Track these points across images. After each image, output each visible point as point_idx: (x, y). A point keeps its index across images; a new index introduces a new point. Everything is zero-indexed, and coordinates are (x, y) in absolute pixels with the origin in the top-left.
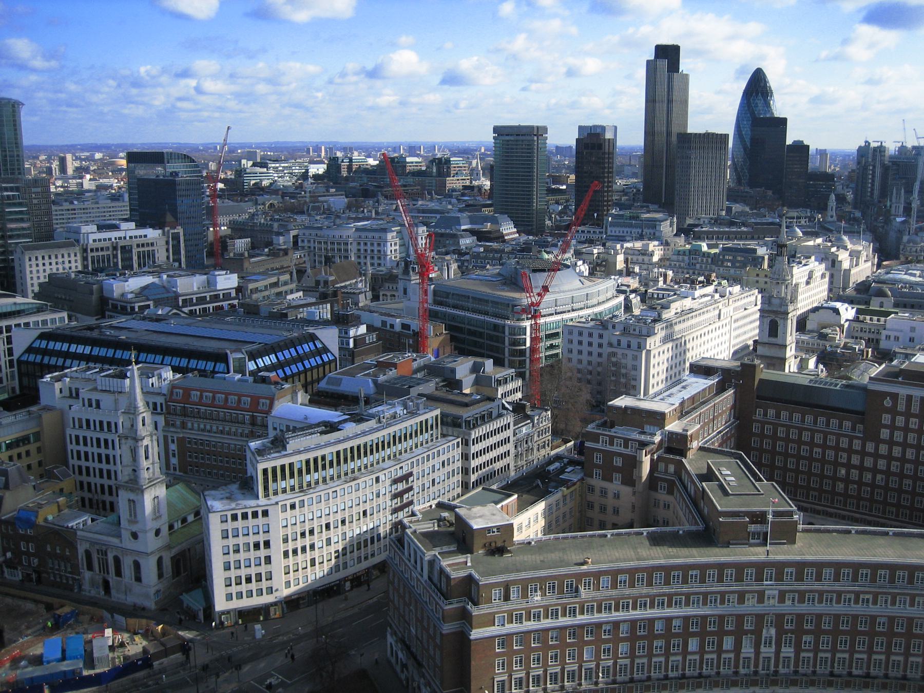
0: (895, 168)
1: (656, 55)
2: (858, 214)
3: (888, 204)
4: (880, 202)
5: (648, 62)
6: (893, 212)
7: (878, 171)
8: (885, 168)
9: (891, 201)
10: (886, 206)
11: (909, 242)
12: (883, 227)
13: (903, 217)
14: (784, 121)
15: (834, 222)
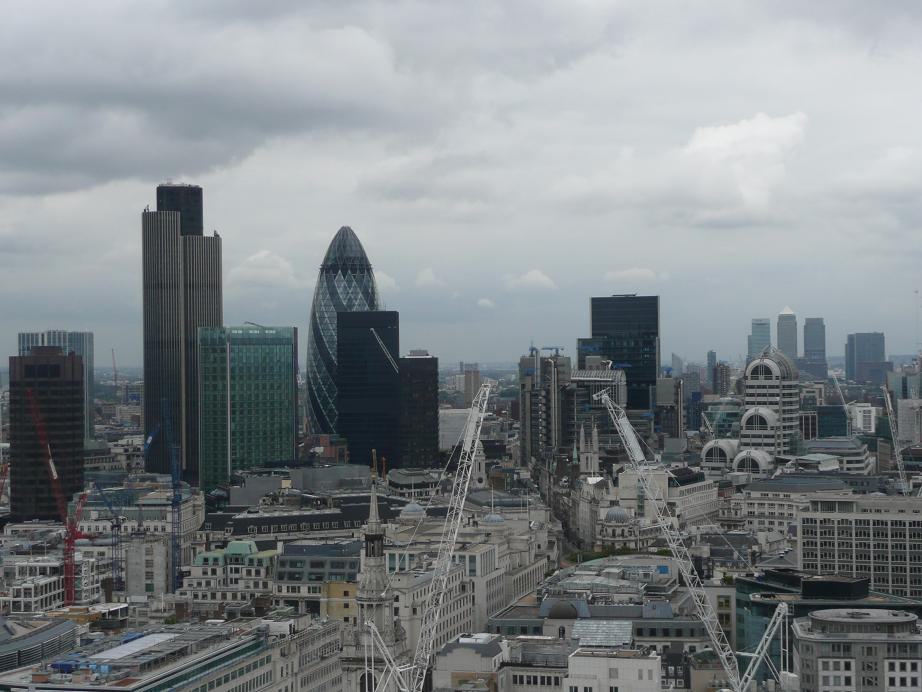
0: (582, 391)
1: (160, 205)
2: (525, 475)
3: (575, 456)
4: (561, 451)
5: (147, 217)
6: (583, 468)
7: (554, 397)
8: (567, 395)
9: (578, 449)
10: (571, 459)
11: (609, 518)
12: (568, 495)
13: (601, 475)
14: (392, 318)
15: (484, 489)
